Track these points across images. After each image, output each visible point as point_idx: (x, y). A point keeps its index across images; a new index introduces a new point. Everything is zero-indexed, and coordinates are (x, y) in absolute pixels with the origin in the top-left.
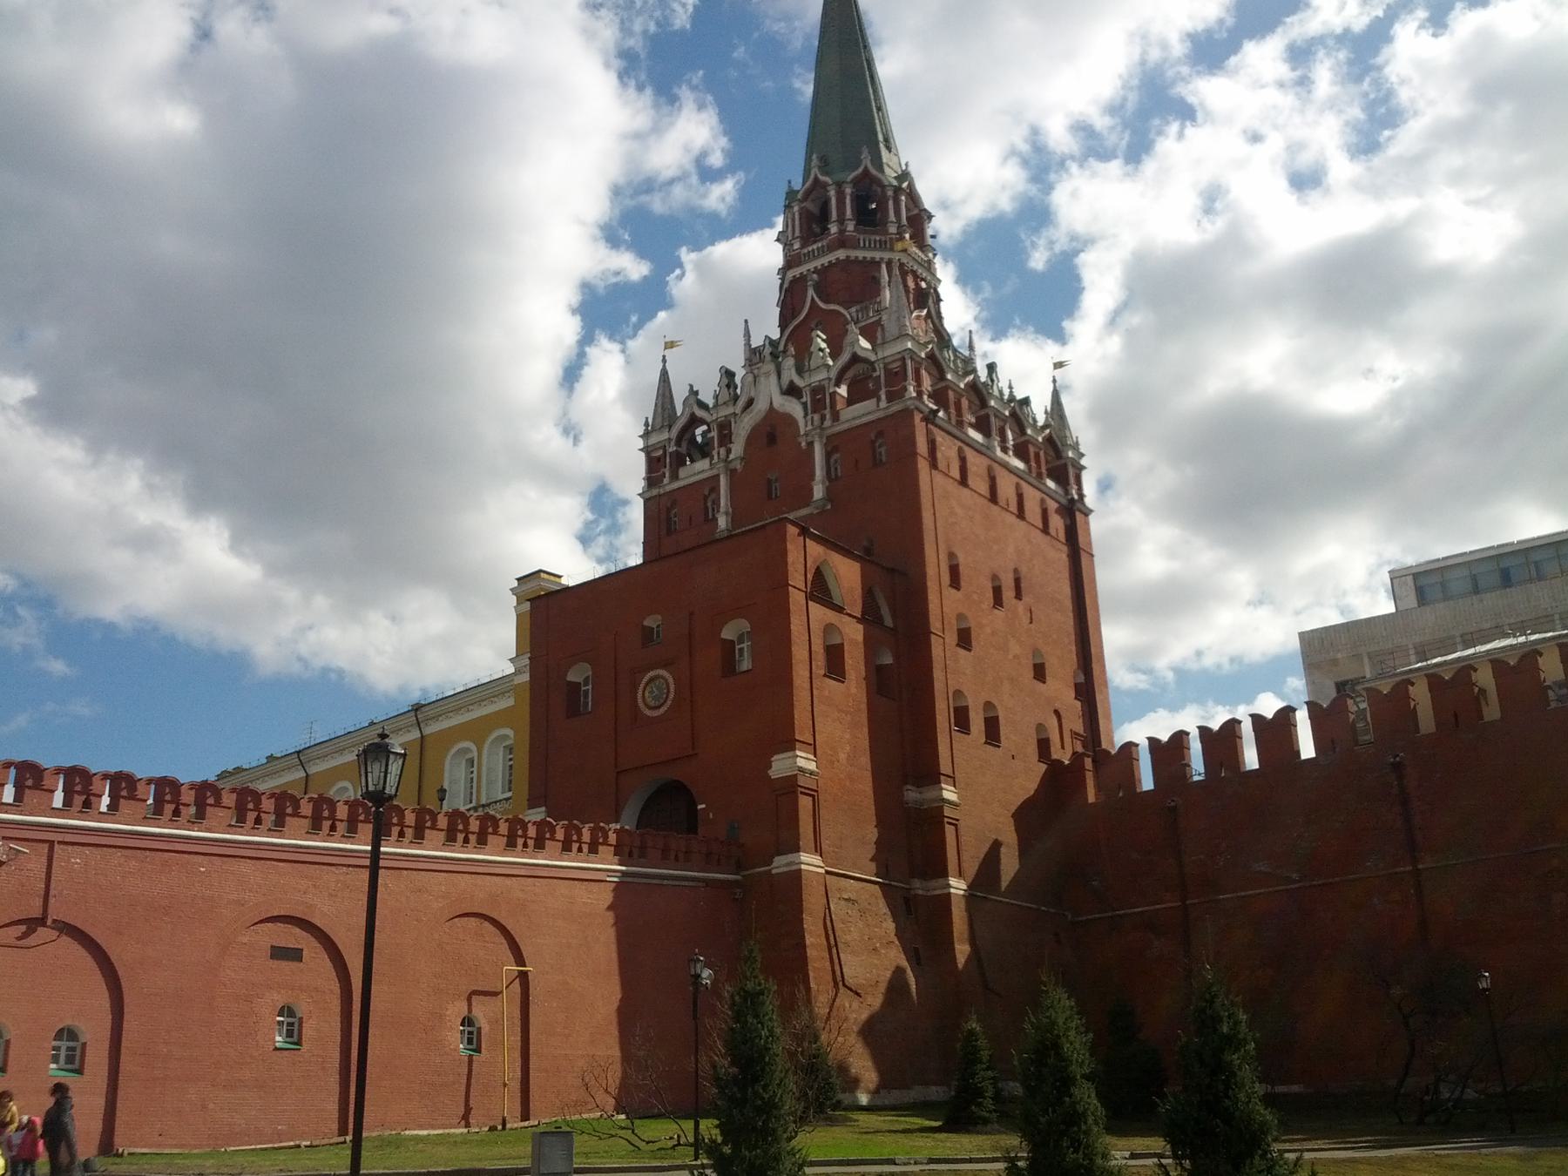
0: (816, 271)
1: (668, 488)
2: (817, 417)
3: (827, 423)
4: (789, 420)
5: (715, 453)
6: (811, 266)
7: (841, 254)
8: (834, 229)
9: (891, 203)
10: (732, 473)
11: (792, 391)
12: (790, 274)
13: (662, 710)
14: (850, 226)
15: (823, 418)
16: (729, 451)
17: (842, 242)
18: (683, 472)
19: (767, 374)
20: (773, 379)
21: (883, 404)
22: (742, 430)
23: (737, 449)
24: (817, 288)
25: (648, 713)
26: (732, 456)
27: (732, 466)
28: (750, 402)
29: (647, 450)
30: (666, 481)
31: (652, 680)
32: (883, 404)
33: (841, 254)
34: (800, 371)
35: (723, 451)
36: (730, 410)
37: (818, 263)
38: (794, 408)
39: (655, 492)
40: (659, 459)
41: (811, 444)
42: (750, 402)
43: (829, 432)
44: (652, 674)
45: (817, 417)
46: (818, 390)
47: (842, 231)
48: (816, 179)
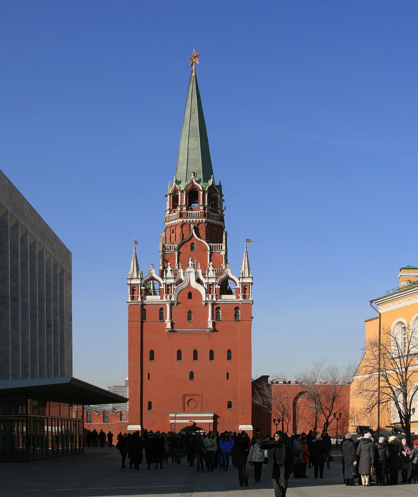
2: (210, 296)
5: (164, 294)
6: (191, 220)
11: (198, 281)
16: (171, 297)
19: (190, 272)
26: (173, 299)
34: (204, 274)
36: (172, 281)
38: (202, 290)
41: (206, 304)
46: (210, 286)
47: (204, 209)
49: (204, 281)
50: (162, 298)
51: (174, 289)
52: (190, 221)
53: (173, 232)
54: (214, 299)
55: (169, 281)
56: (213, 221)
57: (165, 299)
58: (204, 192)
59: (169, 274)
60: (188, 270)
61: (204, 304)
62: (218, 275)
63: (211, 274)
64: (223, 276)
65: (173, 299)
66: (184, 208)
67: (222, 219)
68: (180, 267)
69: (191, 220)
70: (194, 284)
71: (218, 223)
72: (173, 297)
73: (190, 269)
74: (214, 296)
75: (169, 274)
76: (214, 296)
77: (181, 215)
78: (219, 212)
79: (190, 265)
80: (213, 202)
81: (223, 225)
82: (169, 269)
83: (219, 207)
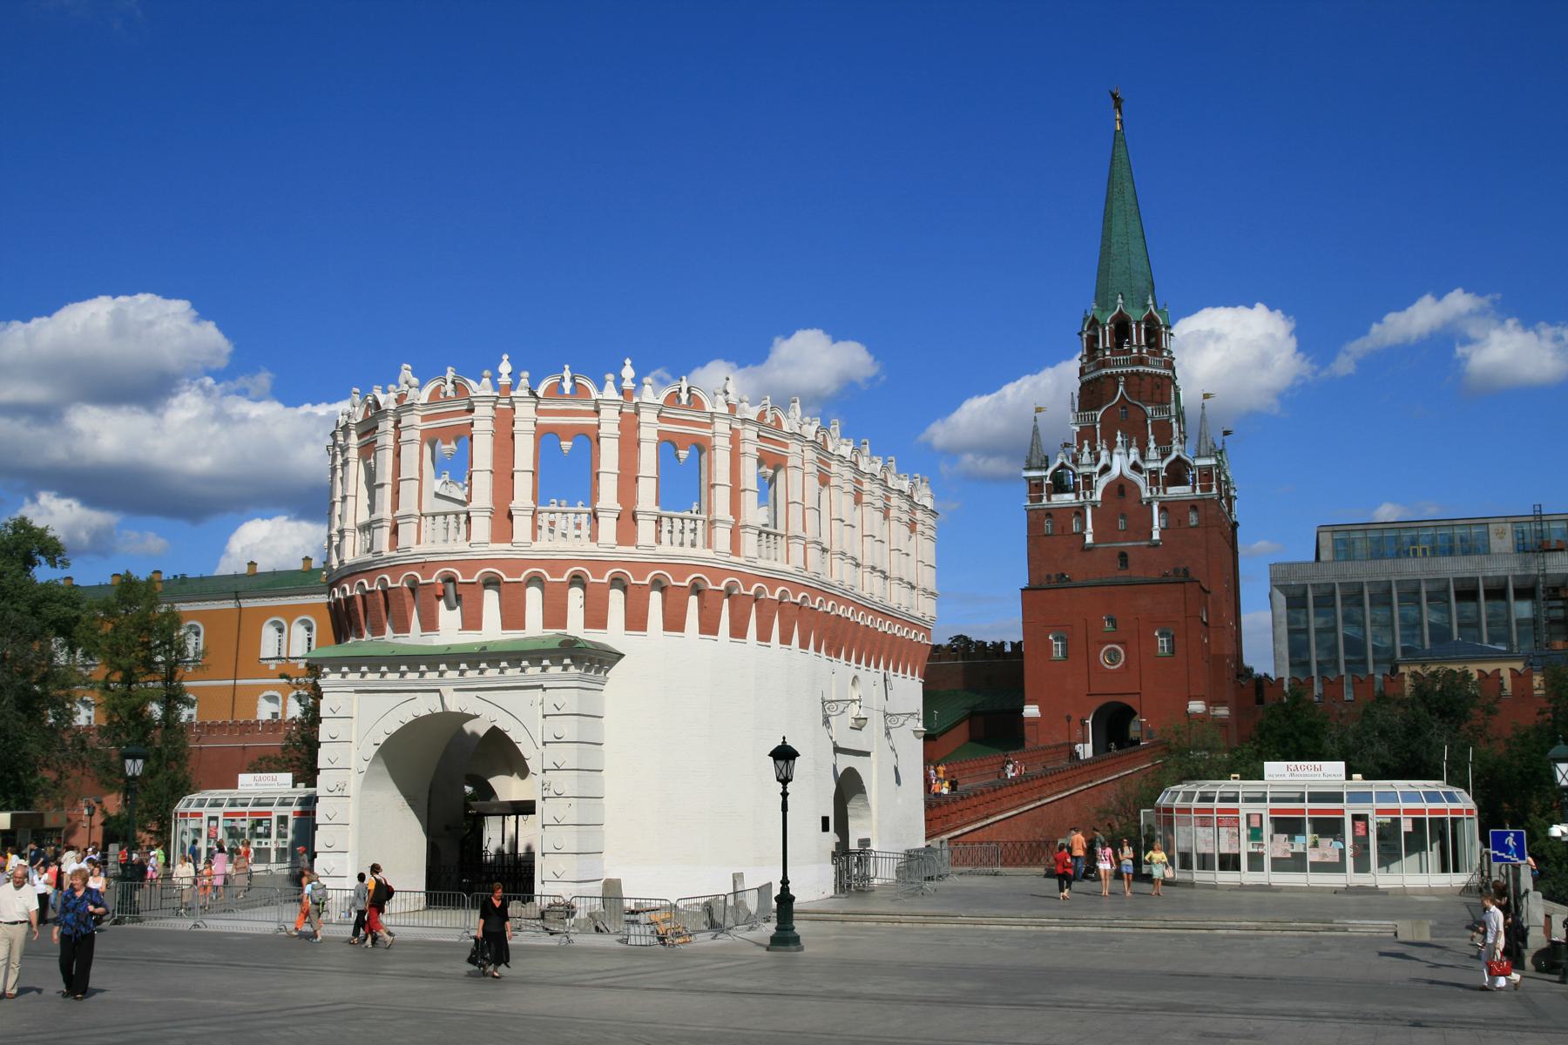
0: (1122, 374)
3: (1161, 494)
4: (1137, 487)
7: (1141, 369)
10: (1094, 507)
17: (1141, 361)
18: (1054, 498)
20: (1124, 457)
21: (1198, 492)
22: (1101, 483)
23: (1098, 496)
24: (1126, 386)
28: (1106, 469)
30: (1045, 501)
32: (1198, 492)
33: (1141, 369)
34: (1143, 456)
39: (1037, 506)
41: (1150, 503)
47: (1140, 352)
54: (1161, 494)
58: (1138, 324)
59: (1086, 459)
62: (1164, 455)
64: (1173, 456)
67: (1169, 365)
70: (1128, 472)
73: (1119, 449)
75: (1086, 459)
77: (1104, 364)
82: (1086, 449)
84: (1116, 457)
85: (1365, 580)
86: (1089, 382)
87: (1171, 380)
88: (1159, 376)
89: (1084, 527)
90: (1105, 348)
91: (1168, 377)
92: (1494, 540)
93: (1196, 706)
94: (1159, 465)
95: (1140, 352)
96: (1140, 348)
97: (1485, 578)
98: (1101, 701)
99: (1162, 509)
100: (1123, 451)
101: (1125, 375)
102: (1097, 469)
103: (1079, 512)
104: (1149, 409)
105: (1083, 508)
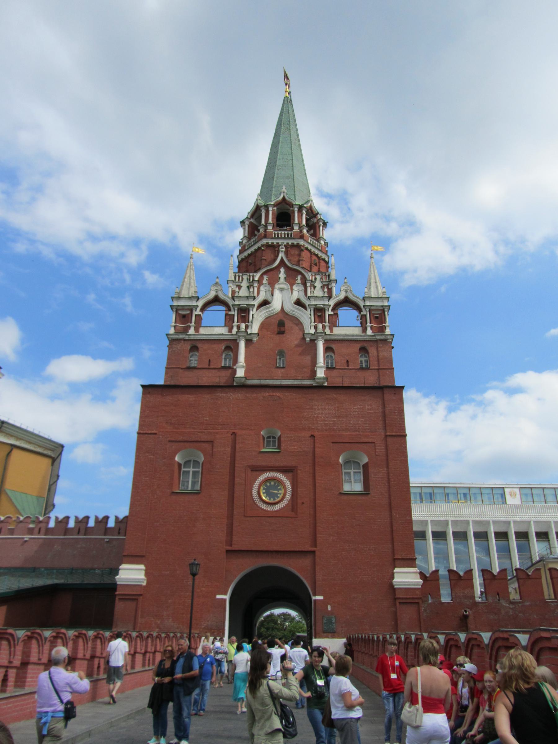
1: (192, 337)
2: (320, 326)
4: (298, 323)
5: (235, 324)
6: (280, 242)
7: (302, 242)
8: (296, 228)
9: (321, 228)
10: (249, 342)
11: (298, 303)
12: (264, 241)
13: (277, 507)
14: (305, 231)
15: (324, 327)
17: (302, 237)
19: (281, 290)
21: (369, 332)
22: (257, 318)
23: (255, 328)
24: (286, 253)
25: (264, 506)
27: (249, 337)
29: (176, 309)
30: (192, 331)
31: (268, 480)
32: (369, 332)
35: (243, 326)
37: (285, 242)
40: (184, 316)
42: (265, 303)
43: (328, 338)
44: (269, 475)
45: (320, 326)
48: (284, 198)
49: (307, 303)
50: (230, 330)
51: (253, 315)
52: (278, 243)
53: (251, 264)
54: (327, 331)
55: (244, 303)
56: (313, 250)
57: (235, 330)
60: (277, 286)
61: (308, 339)
63: (318, 292)
64: (342, 296)
65: (249, 331)
66: (270, 228)
68: (265, 281)
69: (280, 242)
71: (320, 254)
72: (250, 327)
74: (327, 328)
76: (327, 328)
78: (322, 242)
79: (282, 280)
80: (312, 232)
81: (327, 259)
83: (321, 235)
84: (277, 293)
85: (429, 519)
86: (249, 255)
87: (327, 263)
88: (317, 255)
89: (236, 361)
90: (266, 226)
91: (324, 260)
92: (508, 497)
93: (406, 578)
94: (326, 303)
95: (301, 231)
96: (300, 227)
97: (514, 522)
98: (248, 565)
99: (328, 349)
100: (287, 286)
101: (287, 246)
102: (256, 303)
103: (231, 346)
104: (309, 276)
105: (235, 342)
